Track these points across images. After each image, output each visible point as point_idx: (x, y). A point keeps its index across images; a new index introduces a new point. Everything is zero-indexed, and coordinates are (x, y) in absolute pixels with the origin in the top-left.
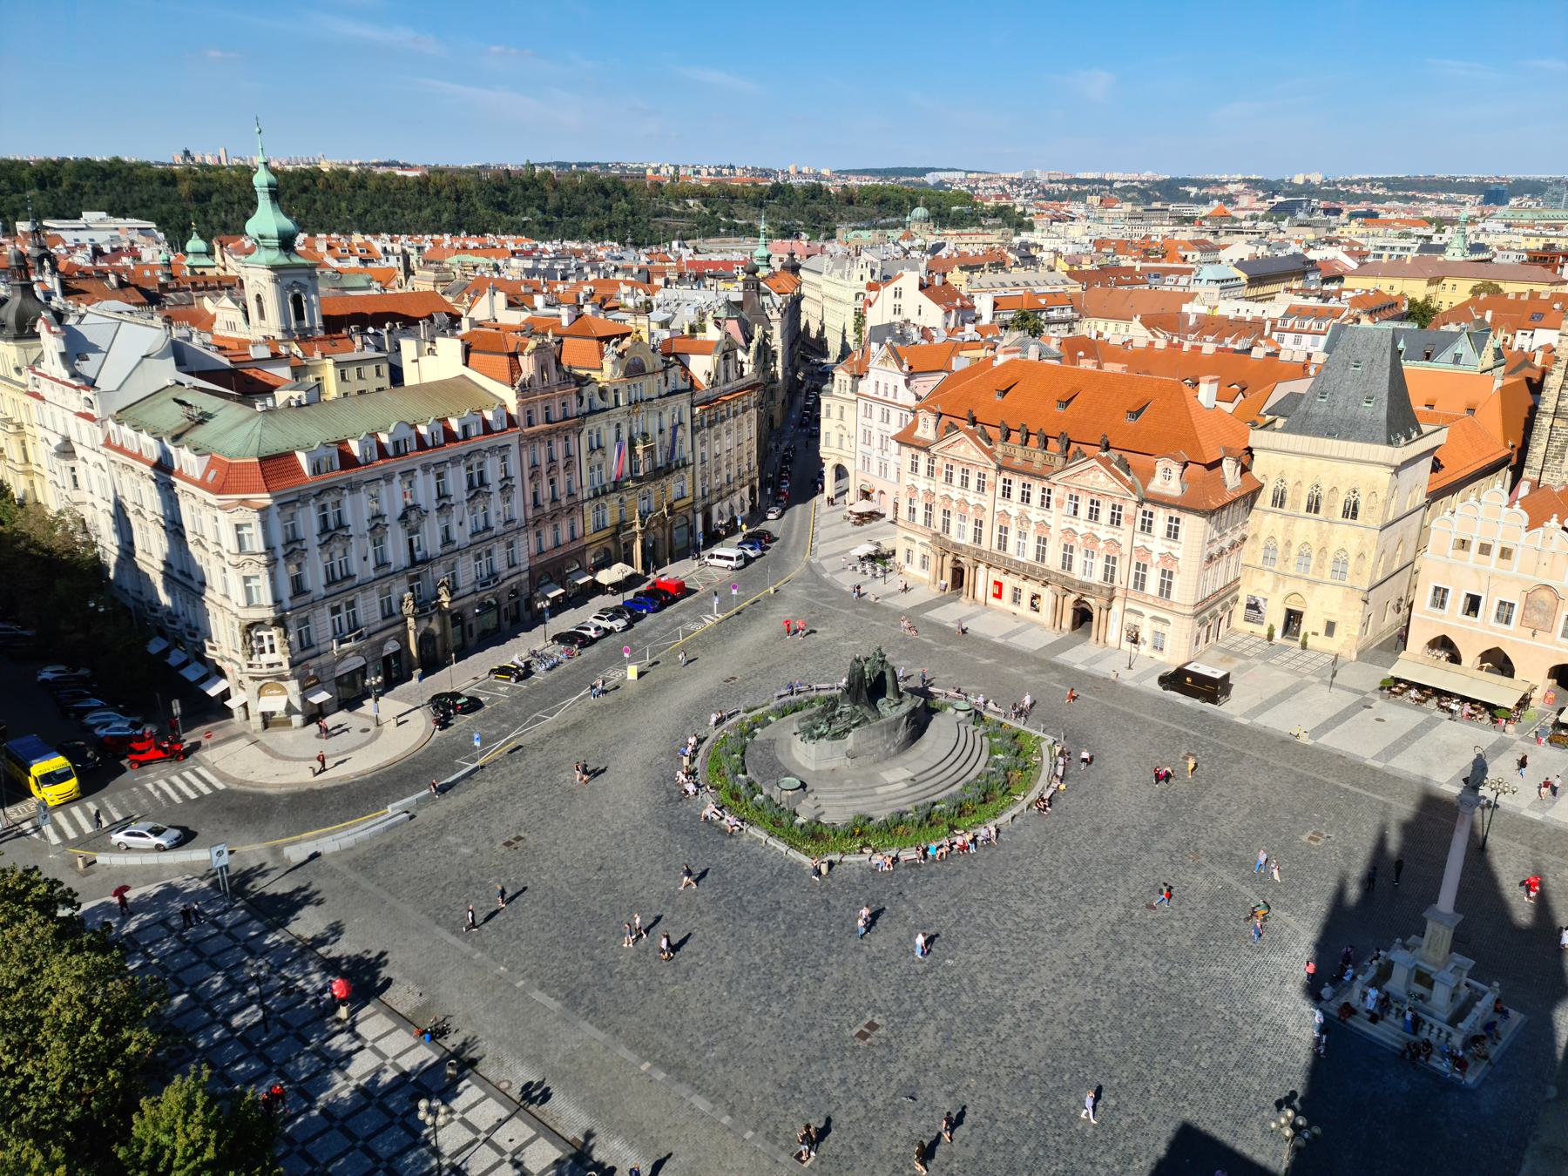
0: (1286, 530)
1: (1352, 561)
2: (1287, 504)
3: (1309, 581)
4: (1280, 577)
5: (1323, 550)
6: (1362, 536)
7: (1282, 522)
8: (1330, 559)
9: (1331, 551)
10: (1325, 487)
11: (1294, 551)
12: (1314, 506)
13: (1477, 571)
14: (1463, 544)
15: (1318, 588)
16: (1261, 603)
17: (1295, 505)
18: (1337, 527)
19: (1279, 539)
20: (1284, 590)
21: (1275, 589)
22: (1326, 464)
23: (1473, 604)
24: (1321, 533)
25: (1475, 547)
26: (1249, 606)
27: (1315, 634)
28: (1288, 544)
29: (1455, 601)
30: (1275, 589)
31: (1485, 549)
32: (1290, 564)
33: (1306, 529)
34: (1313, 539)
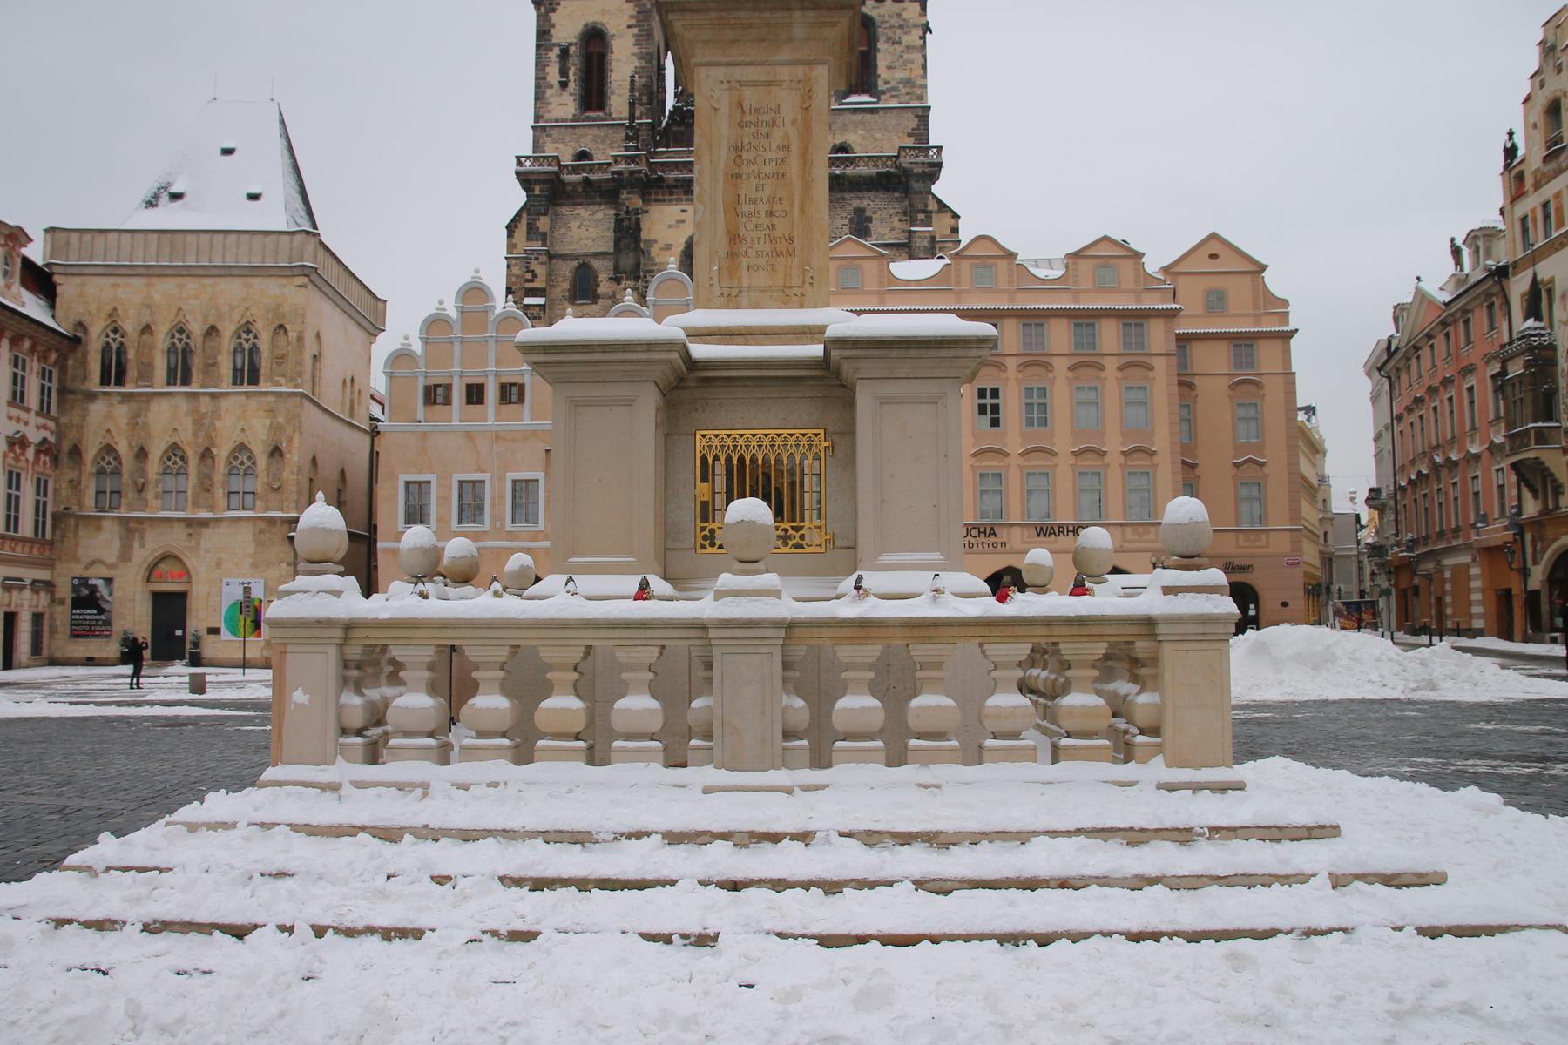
0: (133, 424)
1: (262, 461)
2: (132, 373)
3: (189, 523)
4: (132, 529)
5: (206, 454)
6: (271, 412)
7: (122, 411)
8: (221, 467)
9: (222, 453)
10: (197, 328)
11: (154, 466)
12: (180, 372)
13: (469, 435)
14: (435, 395)
15: (206, 532)
16: (103, 590)
17: (146, 375)
18: (225, 404)
19: (123, 448)
20: (143, 554)
21: (125, 555)
22: (192, 285)
23: (471, 505)
24: (198, 423)
25: (458, 395)
26: (78, 603)
27: (214, 631)
28: (142, 454)
29: (444, 500)
30: (125, 555)
31: (475, 394)
32: (150, 495)
33: (169, 419)
34: (186, 437)
